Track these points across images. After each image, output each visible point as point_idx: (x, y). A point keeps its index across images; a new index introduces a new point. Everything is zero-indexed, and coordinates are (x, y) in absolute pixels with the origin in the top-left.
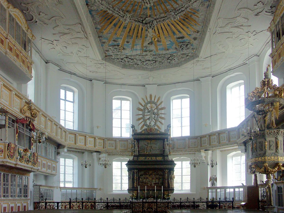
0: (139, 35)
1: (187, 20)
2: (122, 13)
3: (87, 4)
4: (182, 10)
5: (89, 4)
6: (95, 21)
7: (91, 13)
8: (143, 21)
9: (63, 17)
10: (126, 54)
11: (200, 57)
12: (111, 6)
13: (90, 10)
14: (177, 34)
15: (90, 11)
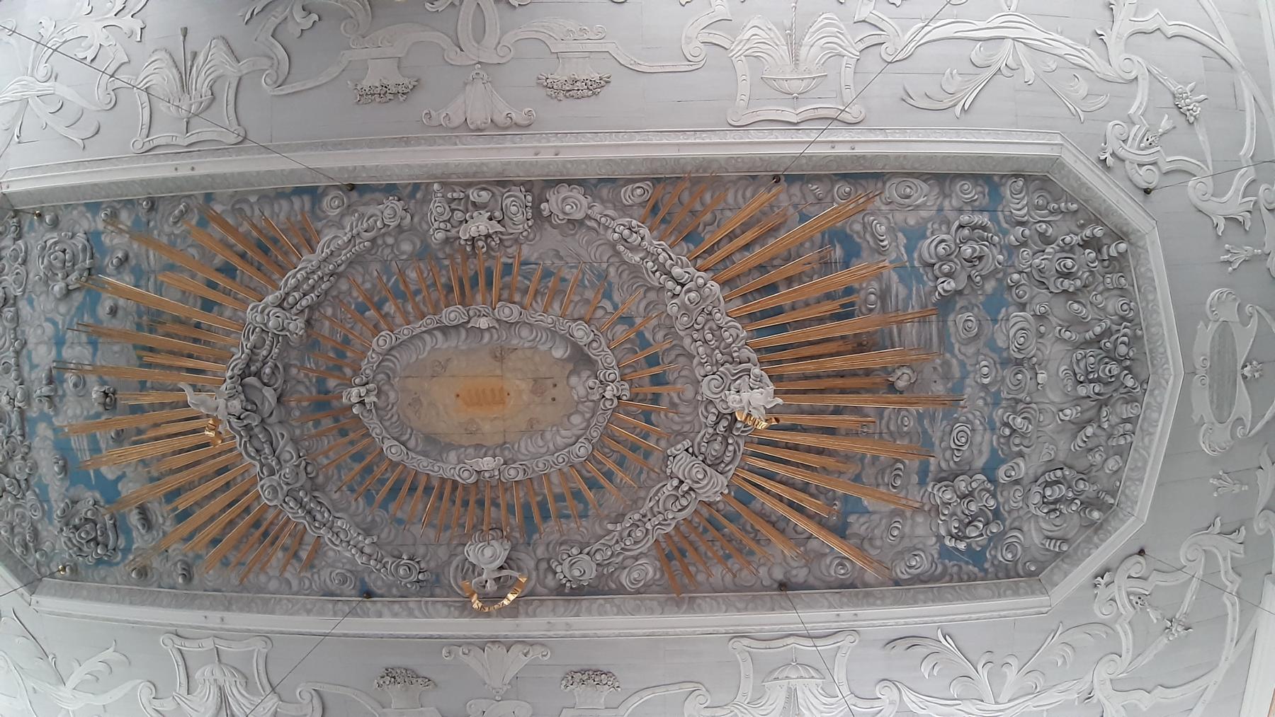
0: (150, 358)
1: (258, 533)
2: (304, 303)
3: (352, 187)
4: (314, 513)
5: (354, 194)
6: (253, 199)
7: (299, 191)
8: (258, 374)
9: (287, 89)
10: (31, 302)
11: (34, 598)
12: (342, 268)
13: (320, 191)
14: (174, 505)
15: (314, 193)
